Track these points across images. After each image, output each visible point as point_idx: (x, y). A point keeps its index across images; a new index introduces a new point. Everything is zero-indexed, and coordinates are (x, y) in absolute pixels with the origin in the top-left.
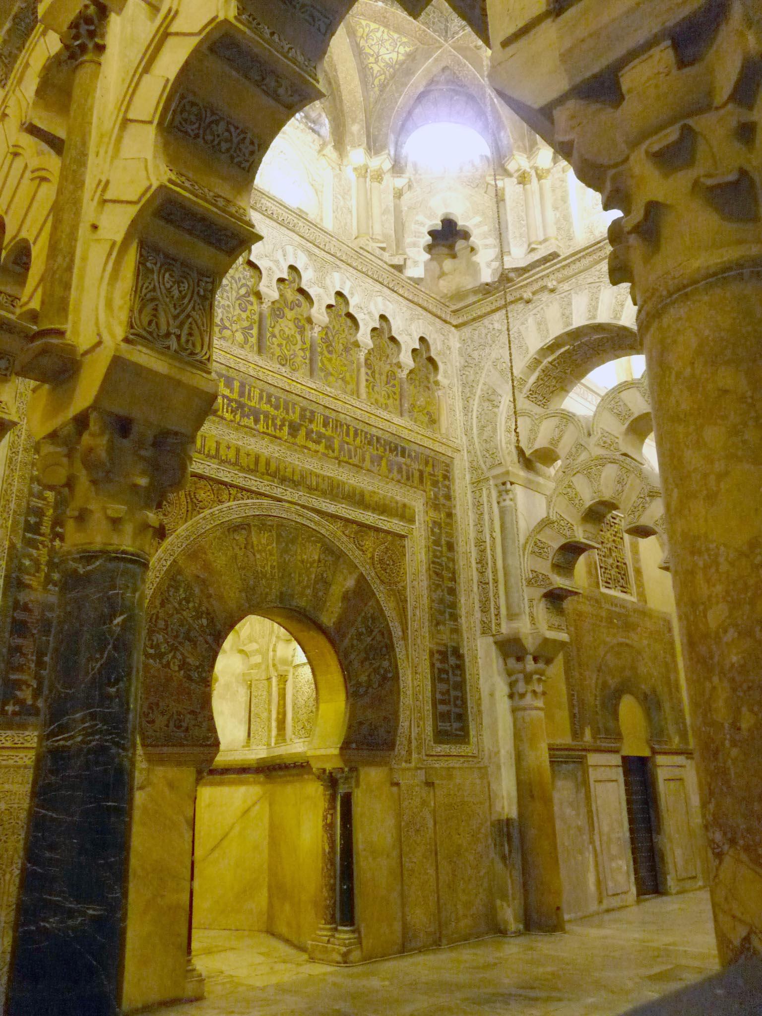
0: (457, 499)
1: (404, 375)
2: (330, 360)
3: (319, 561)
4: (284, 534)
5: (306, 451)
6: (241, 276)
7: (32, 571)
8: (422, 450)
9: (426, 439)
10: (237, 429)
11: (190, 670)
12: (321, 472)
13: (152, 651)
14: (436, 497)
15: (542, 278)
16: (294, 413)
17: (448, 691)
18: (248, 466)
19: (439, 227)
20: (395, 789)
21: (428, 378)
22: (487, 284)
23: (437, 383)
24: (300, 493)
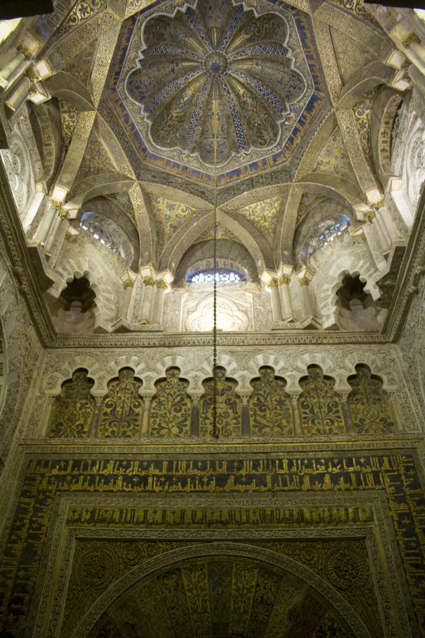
1: (344, 399)
2: (264, 417)
3: (258, 585)
4: (216, 570)
5: (235, 494)
6: (176, 390)
8: (374, 453)
9: (375, 442)
12: (252, 506)
14: (399, 489)
15: (410, 270)
16: (221, 467)
18: (174, 522)
19: (341, 285)
21: (376, 392)
22: (379, 300)
23: (385, 392)
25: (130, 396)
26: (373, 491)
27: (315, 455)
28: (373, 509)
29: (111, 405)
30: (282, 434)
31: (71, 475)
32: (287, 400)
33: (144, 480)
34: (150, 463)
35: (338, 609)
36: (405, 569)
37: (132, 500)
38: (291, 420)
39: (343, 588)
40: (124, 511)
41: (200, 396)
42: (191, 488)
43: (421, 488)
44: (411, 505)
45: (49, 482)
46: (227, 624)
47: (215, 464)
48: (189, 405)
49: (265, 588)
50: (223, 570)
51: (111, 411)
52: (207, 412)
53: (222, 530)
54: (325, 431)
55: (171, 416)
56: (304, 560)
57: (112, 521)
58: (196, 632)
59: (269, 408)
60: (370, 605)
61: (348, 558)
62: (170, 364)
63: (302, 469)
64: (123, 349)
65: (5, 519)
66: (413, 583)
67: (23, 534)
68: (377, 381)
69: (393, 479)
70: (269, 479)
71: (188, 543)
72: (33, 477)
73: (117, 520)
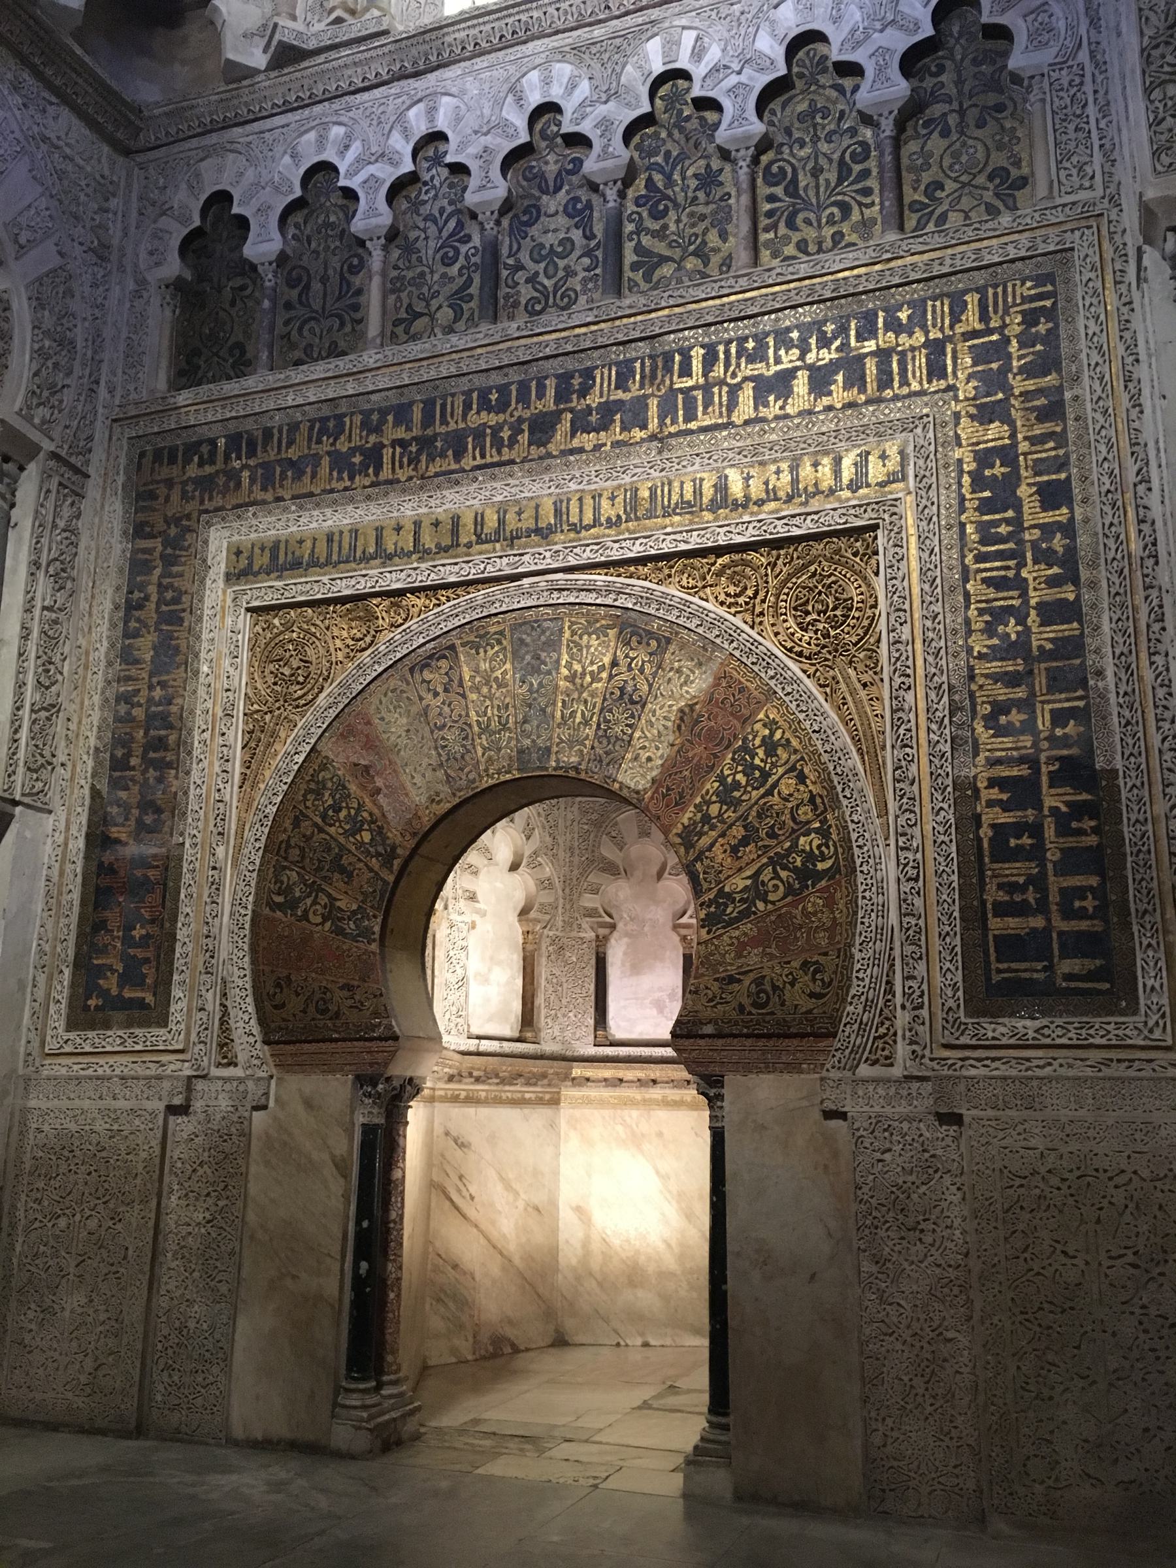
0: (1083, 356)
1: (888, 127)
2: (660, 234)
3: (614, 663)
4: (528, 640)
5: (572, 458)
7: (121, 820)
9: (950, 251)
10: (421, 488)
11: (340, 919)
13: (279, 899)
14: (994, 381)
16: (541, 395)
17: (1038, 882)
20: (834, 1123)
23: (1016, 78)
24: (556, 548)
25: (338, 243)
26: (918, 400)
27: (777, 320)
28: (910, 449)
29: (300, 279)
30: (704, 276)
31: (225, 472)
32: (728, 168)
33: (373, 457)
34: (384, 413)
35: (787, 699)
36: (967, 595)
37: (350, 508)
38: (730, 228)
39: (806, 653)
40: (336, 538)
41: (496, 206)
42: (474, 458)
43: (1059, 371)
44: (1019, 423)
45: (184, 496)
46: (548, 750)
47: (529, 388)
48: (476, 240)
49: (630, 669)
50: (543, 638)
51: (300, 295)
52: (519, 249)
53: (541, 550)
54: (820, 244)
55: (436, 277)
56: (722, 597)
57: (314, 563)
58: (486, 770)
59: (676, 205)
60: (865, 685)
61: (833, 578)
62: (421, 128)
63: (738, 365)
64: (307, 112)
65: (110, 591)
66: (982, 625)
67: (150, 612)
68: (1001, 44)
69: (981, 356)
70: (653, 404)
71: (470, 589)
72: (151, 491)
73: (322, 560)
